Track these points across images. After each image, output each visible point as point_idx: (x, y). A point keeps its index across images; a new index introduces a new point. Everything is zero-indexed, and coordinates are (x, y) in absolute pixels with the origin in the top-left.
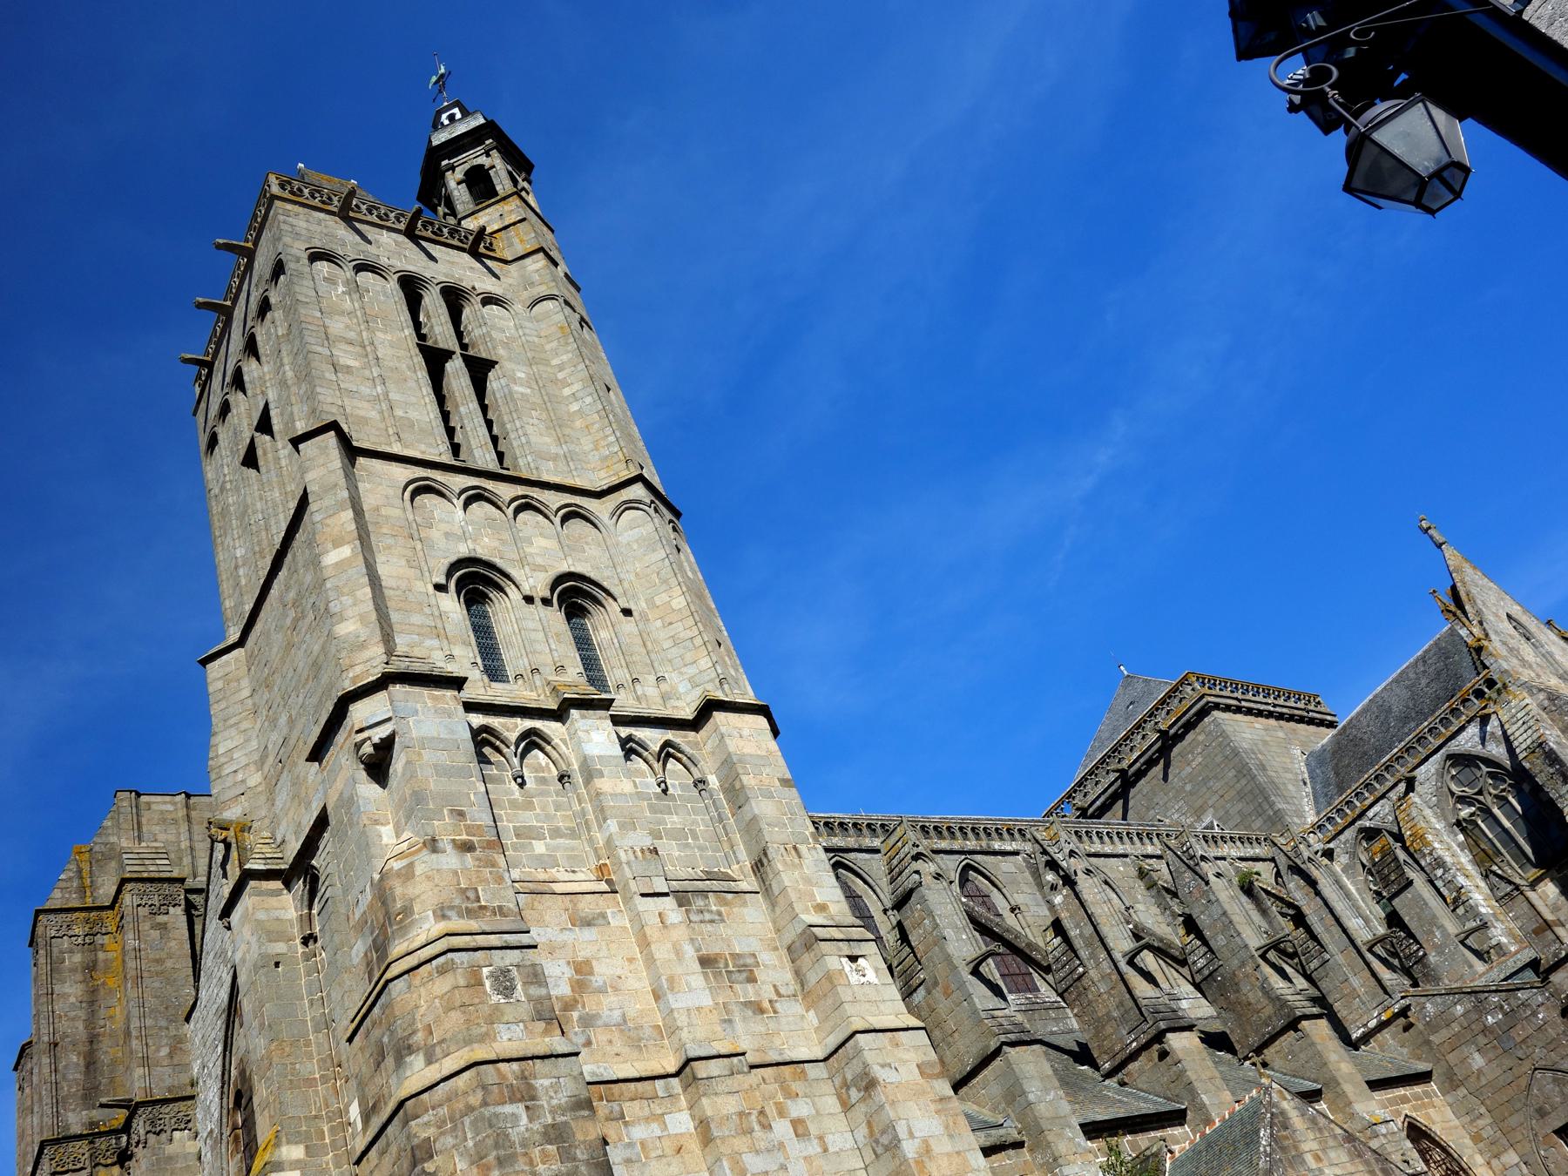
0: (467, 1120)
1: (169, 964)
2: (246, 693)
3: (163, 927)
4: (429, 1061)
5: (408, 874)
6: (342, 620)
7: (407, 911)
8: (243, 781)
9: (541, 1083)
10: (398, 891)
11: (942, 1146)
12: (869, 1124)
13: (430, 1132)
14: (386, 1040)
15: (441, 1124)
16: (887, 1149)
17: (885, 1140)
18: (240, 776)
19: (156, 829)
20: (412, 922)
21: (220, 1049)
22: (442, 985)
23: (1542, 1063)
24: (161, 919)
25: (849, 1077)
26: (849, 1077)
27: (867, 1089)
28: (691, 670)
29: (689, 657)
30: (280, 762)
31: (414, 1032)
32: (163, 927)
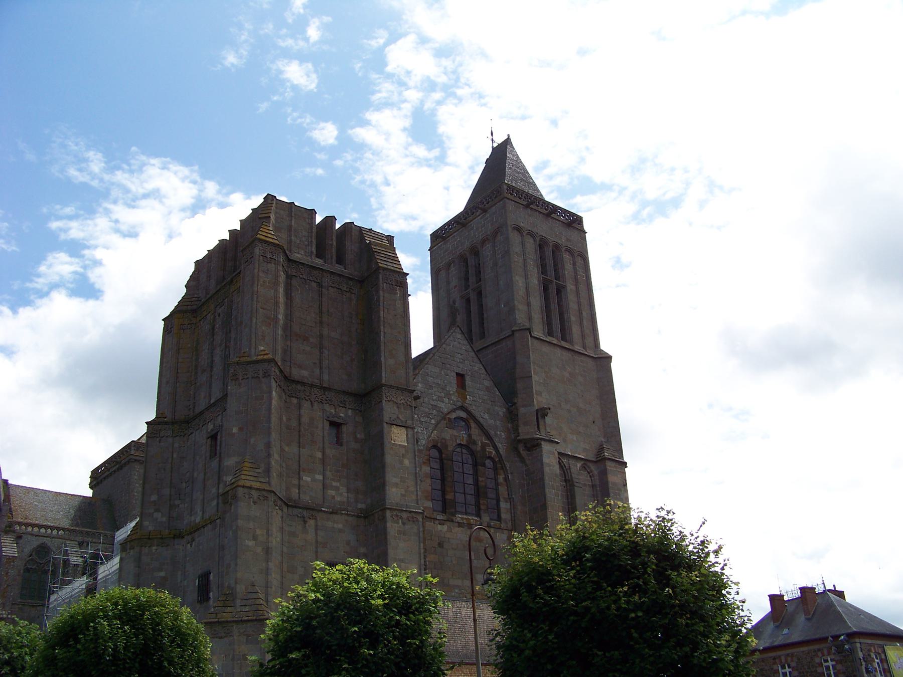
21: (433, 421)
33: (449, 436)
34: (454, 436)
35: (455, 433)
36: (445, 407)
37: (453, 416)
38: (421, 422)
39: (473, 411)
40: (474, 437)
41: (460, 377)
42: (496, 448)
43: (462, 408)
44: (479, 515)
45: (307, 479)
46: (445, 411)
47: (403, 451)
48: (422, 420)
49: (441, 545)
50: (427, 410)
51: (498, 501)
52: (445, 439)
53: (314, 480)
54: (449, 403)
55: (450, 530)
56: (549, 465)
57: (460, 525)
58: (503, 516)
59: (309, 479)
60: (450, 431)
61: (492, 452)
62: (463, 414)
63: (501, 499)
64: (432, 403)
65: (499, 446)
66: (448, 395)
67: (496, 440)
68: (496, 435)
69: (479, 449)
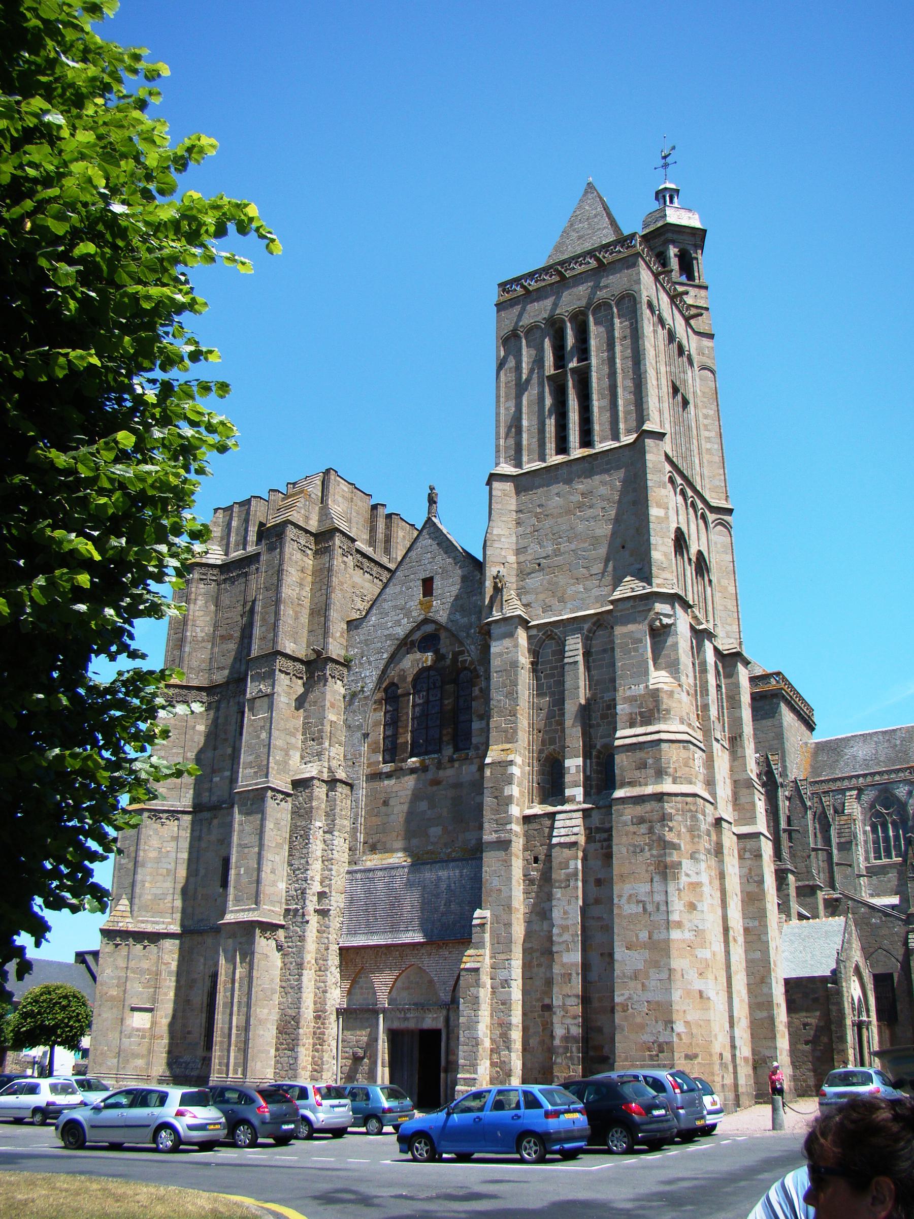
0: (689, 814)
1: (345, 585)
2: (514, 508)
3: (345, 563)
4: (674, 782)
5: (671, 694)
6: (656, 550)
7: (668, 711)
8: (505, 557)
9: (707, 811)
10: (665, 700)
11: (771, 891)
12: (750, 869)
13: (673, 811)
14: (650, 761)
15: (678, 810)
16: (755, 882)
17: (756, 879)
18: (503, 553)
19: (340, 499)
20: (670, 718)
21: (385, 656)
22: (684, 754)
23: (885, 947)
24: (345, 558)
25: (748, 847)
26: (748, 847)
27: (755, 856)
28: (728, 628)
29: (729, 620)
30: (539, 565)
32: (345, 563)
35: (418, 655)
36: (400, 632)
37: (418, 635)
38: (370, 663)
44: (439, 751)
45: (217, 779)
49: (386, 803)
51: (471, 721)
52: (403, 670)
53: (222, 779)
56: (500, 654)
59: (218, 779)
61: (466, 660)
63: (474, 718)
64: (386, 632)
69: (448, 662)
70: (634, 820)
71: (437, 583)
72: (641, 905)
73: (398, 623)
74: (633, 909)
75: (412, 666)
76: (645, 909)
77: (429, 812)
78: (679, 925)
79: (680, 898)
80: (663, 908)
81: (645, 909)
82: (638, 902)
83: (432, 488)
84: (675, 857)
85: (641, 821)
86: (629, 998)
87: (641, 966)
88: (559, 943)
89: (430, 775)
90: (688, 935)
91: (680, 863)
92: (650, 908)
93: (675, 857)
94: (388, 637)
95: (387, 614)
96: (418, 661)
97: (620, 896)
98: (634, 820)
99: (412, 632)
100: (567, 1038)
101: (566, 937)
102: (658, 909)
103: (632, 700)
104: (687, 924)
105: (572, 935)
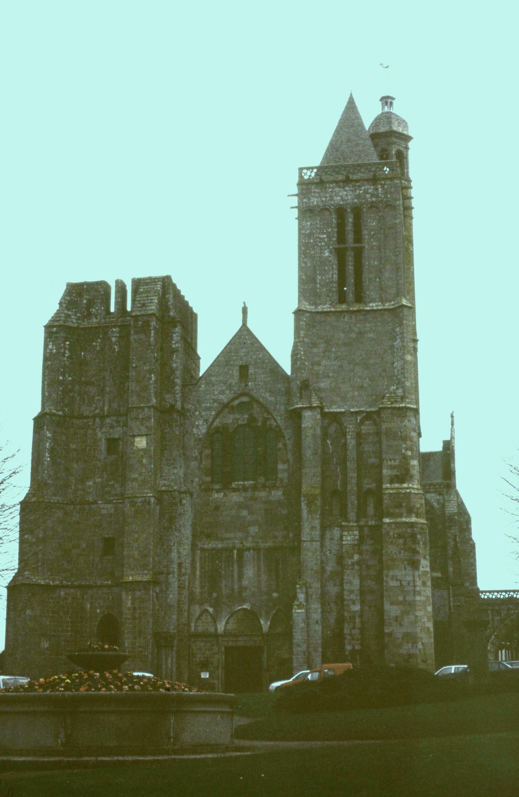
21: (213, 413)
31: (414, 508)
33: (231, 420)
34: (229, 419)
36: (224, 398)
37: (236, 402)
38: (202, 416)
39: (254, 394)
40: (256, 415)
41: (244, 369)
42: (275, 420)
43: (243, 394)
46: (226, 401)
47: (142, 453)
48: (203, 414)
49: (217, 508)
50: (209, 405)
51: (277, 463)
54: (230, 393)
55: (225, 495)
57: (235, 490)
58: (280, 476)
60: (232, 416)
61: (273, 424)
62: (245, 399)
63: (279, 462)
64: (214, 397)
65: (278, 419)
66: (230, 387)
67: (275, 414)
68: (275, 409)
69: (260, 424)
70: (395, 536)
71: (251, 370)
72: (399, 582)
73: (222, 392)
74: (393, 583)
75: (233, 423)
76: (401, 584)
77: (249, 517)
78: (419, 593)
79: (420, 579)
80: (412, 584)
81: (401, 584)
82: (397, 580)
83: (244, 303)
84: (417, 557)
85: (400, 536)
86: (393, 631)
87: (398, 613)
88: (348, 600)
89: (249, 494)
90: (423, 598)
91: (420, 561)
92: (404, 583)
93: (417, 557)
94: (215, 401)
95: (213, 385)
96: (238, 419)
97: (387, 576)
98: (395, 536)
99: (233, 400)
100: (353, 650)
101: (353, 597)
102: (409, 584)
103: (392, 468)
104: (423, 593)
105: (356, 596)
